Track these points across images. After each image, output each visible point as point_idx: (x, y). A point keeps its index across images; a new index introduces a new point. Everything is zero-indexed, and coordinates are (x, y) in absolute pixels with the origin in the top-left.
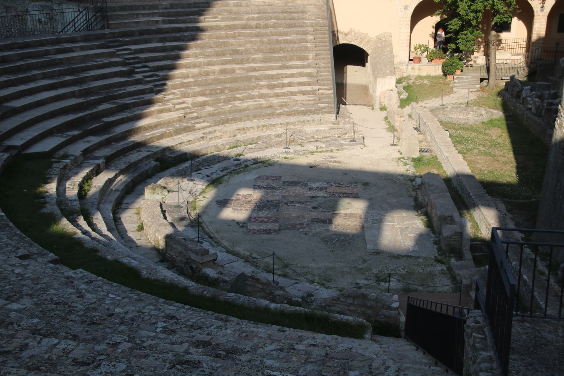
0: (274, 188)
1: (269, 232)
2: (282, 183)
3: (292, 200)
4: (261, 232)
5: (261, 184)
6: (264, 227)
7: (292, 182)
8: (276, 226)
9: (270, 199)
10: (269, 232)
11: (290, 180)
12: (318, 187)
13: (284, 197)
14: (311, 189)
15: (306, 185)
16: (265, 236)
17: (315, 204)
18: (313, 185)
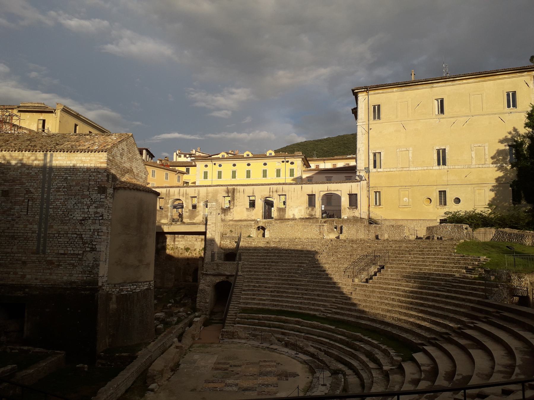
0: (263, 385)
1: (265, 361)
2: (257, 390)
3: (250, 377)
4: (268, 361)
5: (272, 388)
6: (268, 363)
7: (250, 390)
8: (261, 364)
9: (265, 377)
10: (265, 361)
11: (251, 392)
12: (231, 386)
13: (256, 379)
14: (236, 385)
15: (239, 388)
16: (266, 360)
17: (237, 376)
18: (235, 389)
